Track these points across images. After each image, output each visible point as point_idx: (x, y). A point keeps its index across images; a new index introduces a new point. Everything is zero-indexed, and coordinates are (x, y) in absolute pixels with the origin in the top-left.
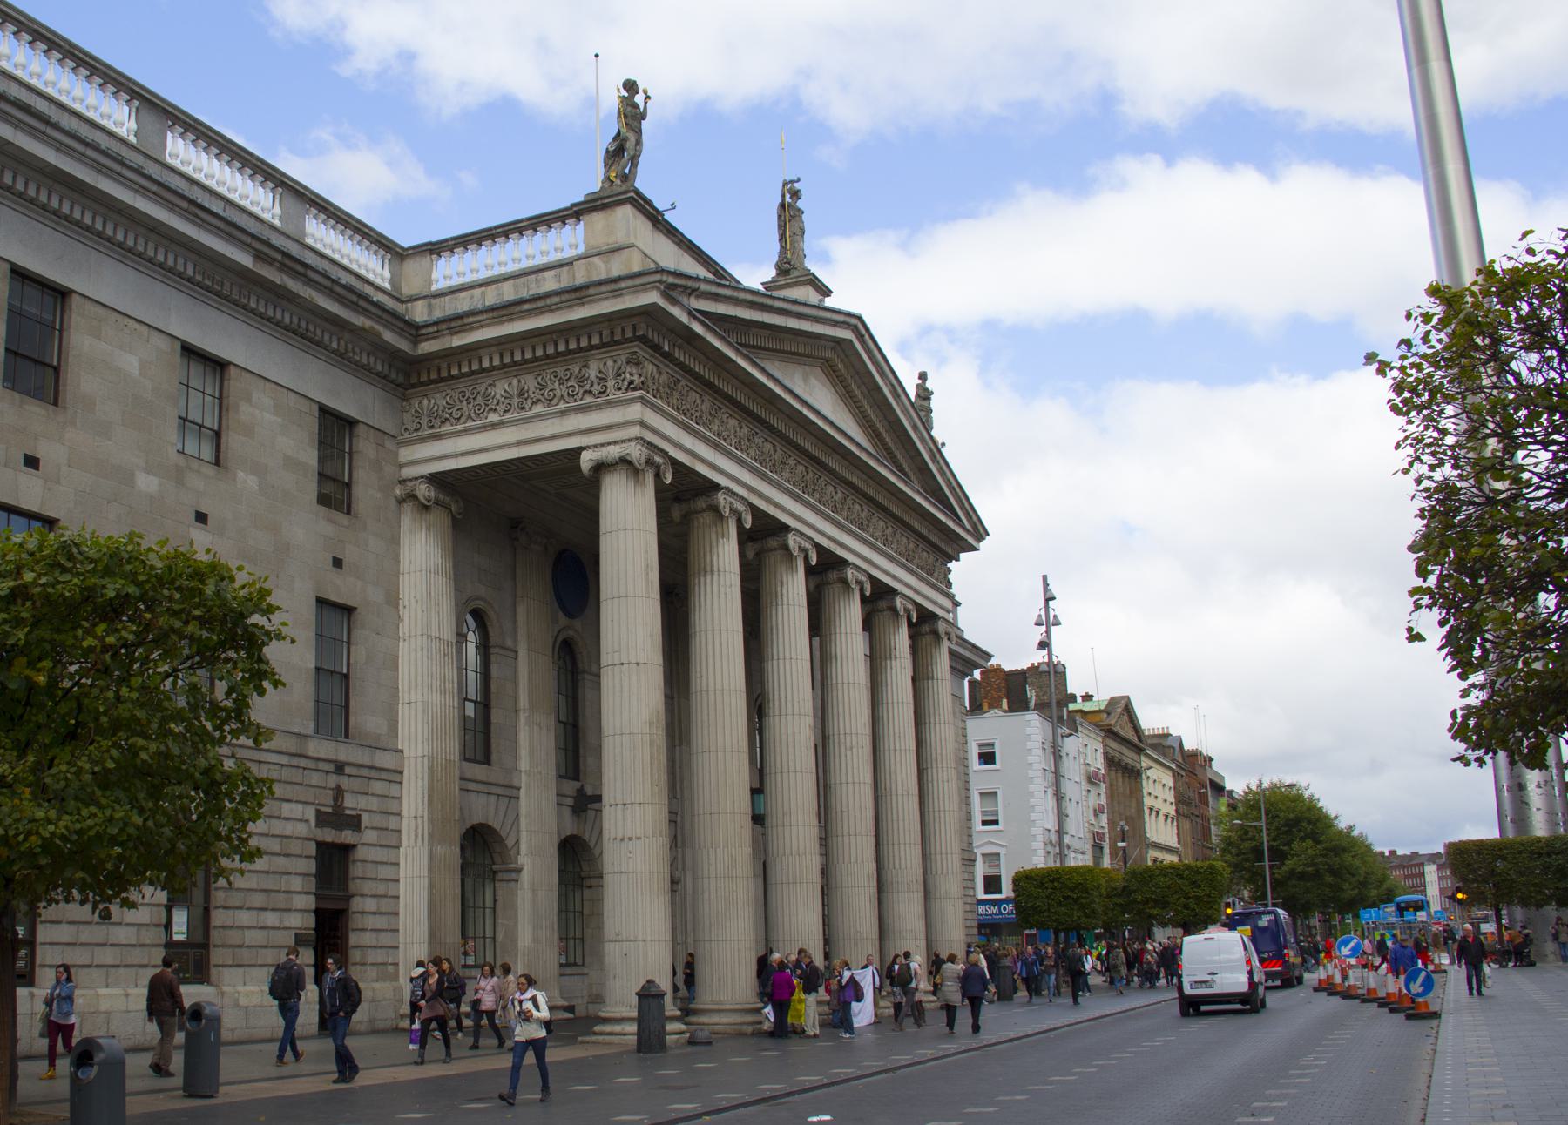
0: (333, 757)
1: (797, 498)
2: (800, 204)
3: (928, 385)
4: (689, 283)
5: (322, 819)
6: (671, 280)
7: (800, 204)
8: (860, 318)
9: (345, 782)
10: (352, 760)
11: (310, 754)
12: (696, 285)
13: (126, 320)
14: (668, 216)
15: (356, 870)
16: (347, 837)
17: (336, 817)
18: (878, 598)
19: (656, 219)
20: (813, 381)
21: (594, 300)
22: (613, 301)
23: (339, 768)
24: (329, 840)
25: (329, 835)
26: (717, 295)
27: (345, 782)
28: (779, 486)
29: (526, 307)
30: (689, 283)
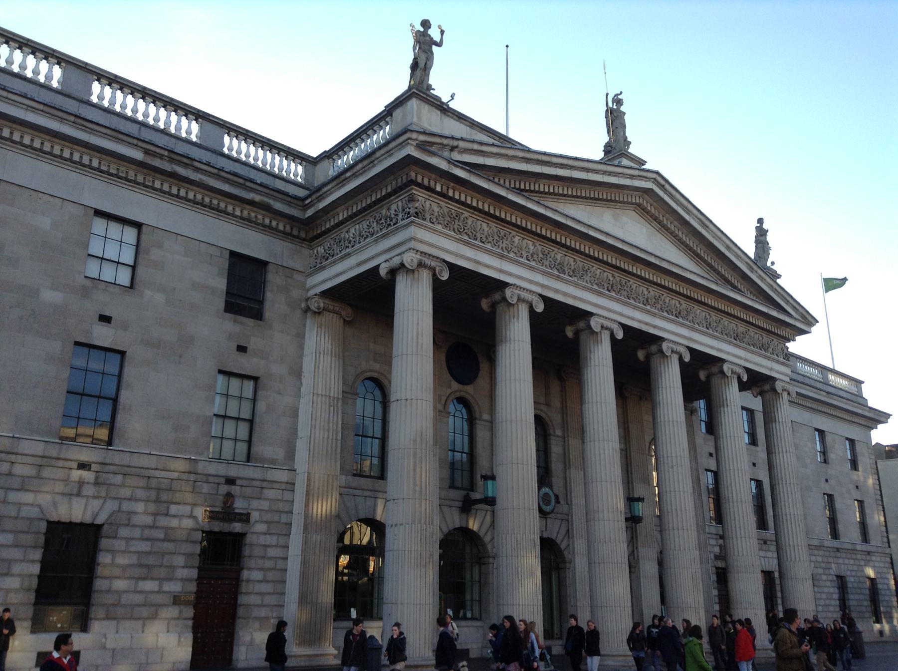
0: (224, 474)
1: (599, 294)
2: (622, 109)
3: (765, 226)
4: (445, 141)
5: (213, 516)
6: (422, 138)
7: (622, 109)
8: (657, 173)
9: (235, 490)
10: (241, 475)
11: (199, 472)
12: (455, 143)
13: (40, 195)
14: (452, 105)
15: (246, 551)
16: (237, 527)
17: (226, 512)
18: (701, 377)
19: (443, 109)
20: (625, 219)
21: (380, 160)
22: (389, 159)
23: (230, 481)
24: (216, 529)
25: (217, 527)
26: (482, 151)
27: (235, 490)
28: (585, 288)
29: (348, 174)
30: (445, 141)
